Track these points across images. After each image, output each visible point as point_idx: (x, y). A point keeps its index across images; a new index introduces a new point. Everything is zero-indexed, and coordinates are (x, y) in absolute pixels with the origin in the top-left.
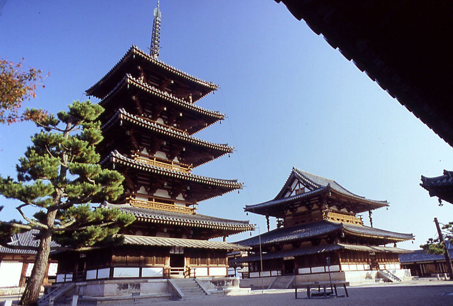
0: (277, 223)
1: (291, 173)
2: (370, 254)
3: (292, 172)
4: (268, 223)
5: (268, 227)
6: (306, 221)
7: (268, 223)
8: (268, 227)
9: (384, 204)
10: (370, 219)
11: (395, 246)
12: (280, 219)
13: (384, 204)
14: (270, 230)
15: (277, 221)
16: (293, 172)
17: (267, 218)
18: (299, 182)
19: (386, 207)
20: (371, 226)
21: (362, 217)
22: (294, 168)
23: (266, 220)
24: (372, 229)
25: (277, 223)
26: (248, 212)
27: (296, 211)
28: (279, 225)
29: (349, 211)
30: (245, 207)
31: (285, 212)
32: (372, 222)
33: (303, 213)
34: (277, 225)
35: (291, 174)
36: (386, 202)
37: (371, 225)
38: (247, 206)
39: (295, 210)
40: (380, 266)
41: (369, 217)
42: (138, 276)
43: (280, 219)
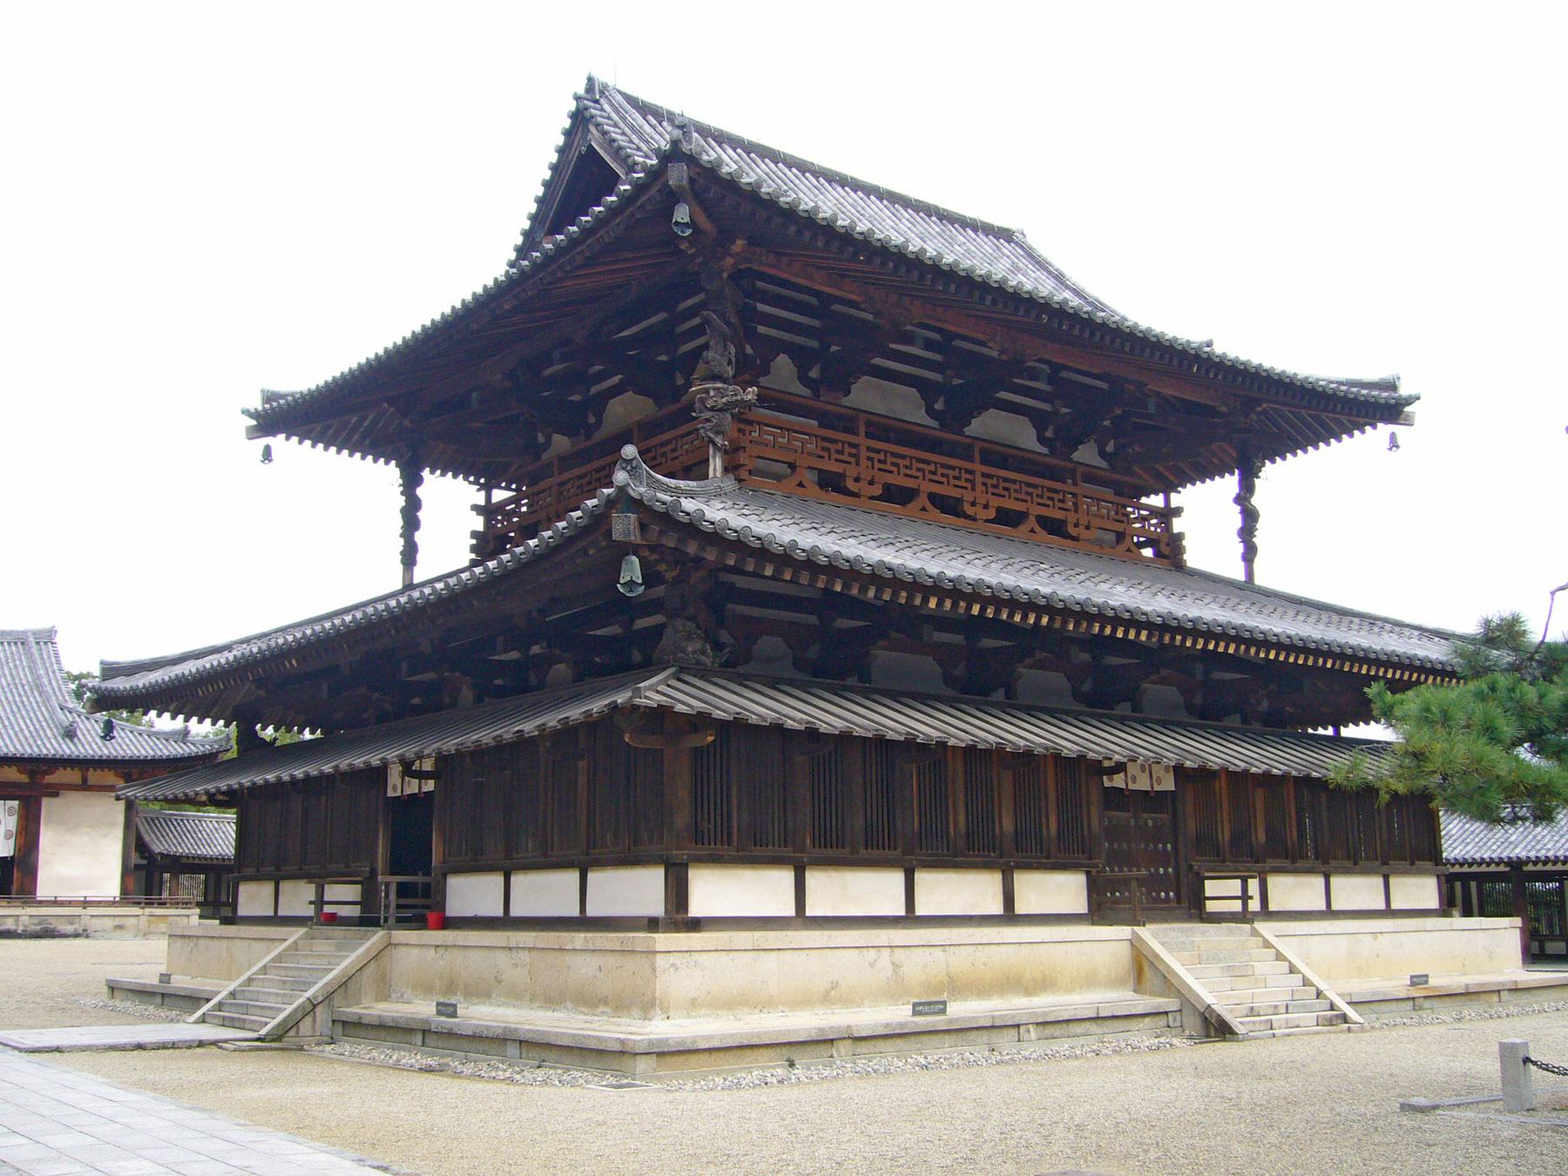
0: (478, 523)
4: (411, 521)
5: (409, 556)
7: (411, 521)
8: (409, 556)
9: (1376, 406)
10: (1237, 522)
12: (499, 495)
13: (1376, 406)
15: (475, 508)
17: (411, 482)
19: (1384, 429)
23: (401, 501)
24: (1247, 590)
25: (478, 523)
26: (278, 442)
27: (599, 423)
28: (487, 545)
29: (1064, 439)
31: (541, 439)
34: (474, 534)
36: (1392, 386)
37: (1242, 565)
39: (592, 420)
42: (903, 913)
43: (499, 495)
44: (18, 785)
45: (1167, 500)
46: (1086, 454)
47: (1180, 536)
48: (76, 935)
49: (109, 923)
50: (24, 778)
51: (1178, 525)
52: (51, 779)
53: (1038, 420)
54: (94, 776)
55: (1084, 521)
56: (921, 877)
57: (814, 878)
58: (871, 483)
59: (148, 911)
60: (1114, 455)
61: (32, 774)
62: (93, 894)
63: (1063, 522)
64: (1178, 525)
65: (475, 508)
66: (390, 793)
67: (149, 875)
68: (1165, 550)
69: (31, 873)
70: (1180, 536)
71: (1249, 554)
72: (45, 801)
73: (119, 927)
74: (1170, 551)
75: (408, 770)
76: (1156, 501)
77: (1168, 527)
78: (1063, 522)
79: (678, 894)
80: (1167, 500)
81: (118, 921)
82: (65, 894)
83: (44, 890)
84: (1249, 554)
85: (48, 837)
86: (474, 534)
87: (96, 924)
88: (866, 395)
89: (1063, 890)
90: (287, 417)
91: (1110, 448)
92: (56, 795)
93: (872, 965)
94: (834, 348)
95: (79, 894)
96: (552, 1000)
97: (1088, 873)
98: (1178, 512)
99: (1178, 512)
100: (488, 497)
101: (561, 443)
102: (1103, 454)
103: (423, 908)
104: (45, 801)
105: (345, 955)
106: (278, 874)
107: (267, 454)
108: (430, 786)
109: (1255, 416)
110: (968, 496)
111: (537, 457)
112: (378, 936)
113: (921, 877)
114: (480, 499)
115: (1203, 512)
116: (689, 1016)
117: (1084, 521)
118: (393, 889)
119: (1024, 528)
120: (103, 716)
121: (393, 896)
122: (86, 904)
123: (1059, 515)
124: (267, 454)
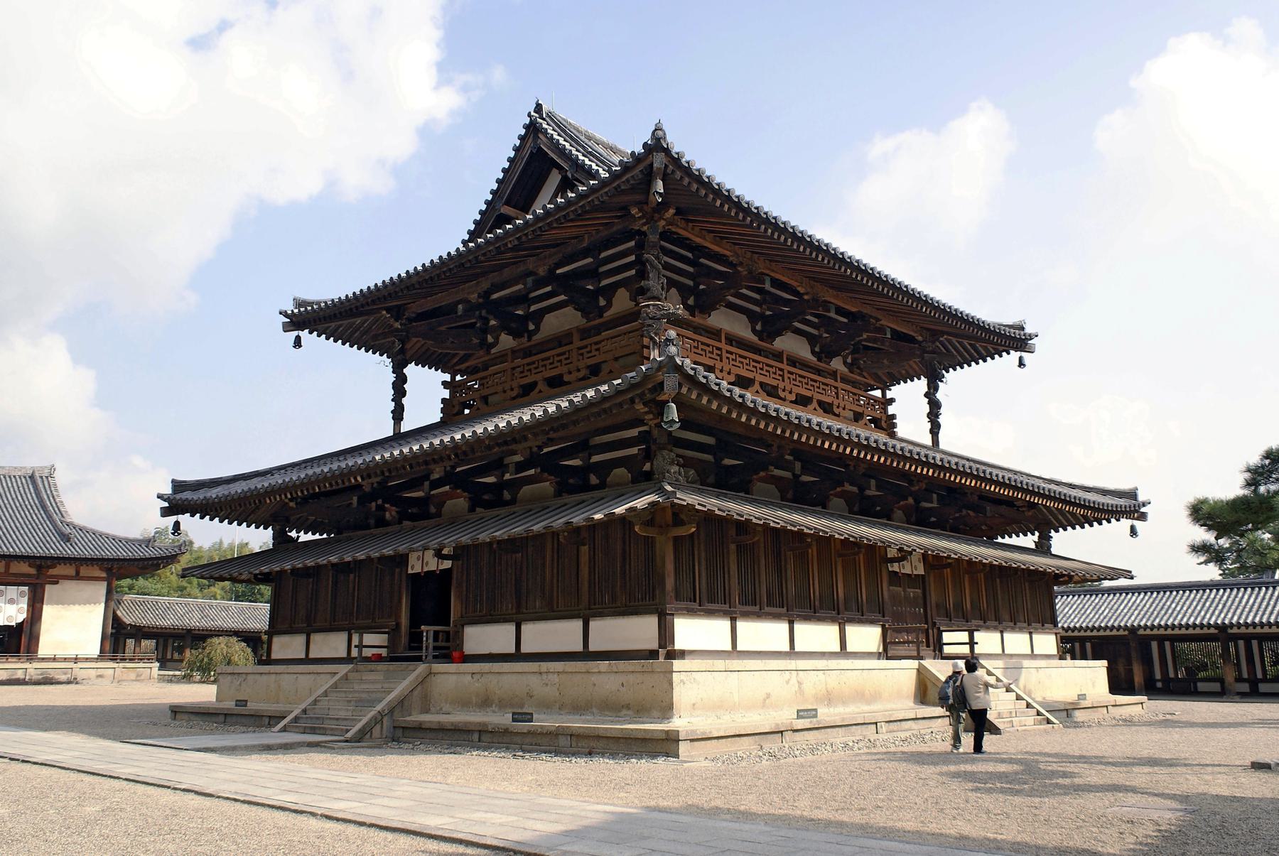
0: (446, 394)
1: (523, 132)
2: (895, 567)
3: (527, 127)
5: (398, 414)
6: (566, 378)
8: (398, 414)
9: (1011, 340)
10: (927, 409)
11: (1043, 547)
13: (1011, 340)
14: (406, 426)
15: (445, 384)
16: (532, 129)
18: (566, 184)
19: (1015, 355)
20: (928, 441)
21: (889, 395)
22: (539, 108)
23: (392, 378)
25: (446, 394)
26: (304, 334)
27: (537, 329)
29: (826, 353)
30: (290, 307)
31: (490, 339)
32: (941, 420)
33: (562, 340)
34: (444, 401)
35: (522, 138)
38: (300, 303)
39: (531, 327)
40: (947, 637)
41: (926, 395)
44: (29, 575)
45: (884, 394)
46: (837, 364)
47: (893, 416)
48: (69, 682)
49: (93, 673)
50: (33, 571)
51: (891, 410)
52: (52, 572)
53: (812, 340)
54: (84, 571)
55: (842, 405)
56: (798, 627)
57: (742, 625)
58: (729, 373)
60: (852, 364)
61: (39, 568)
62: (82, 653)
63: (831, 405)
64: (891, 410)
65: (445, 384)
66: (410, 571)
67: (119, 638)
68: (884, 425)
69: (34, 639)
70: (893, 416)
71: (935, 429)
72: (48, 587)
73: (100, 676)
74: (887, 424)
75: (439, 555)
76: (877, 393)
77: (885, 410)
78: (831, 405)
79: (666, 634)
80: (884, 394)
81: (100, 672)
82: (60, 653)
83: (44, 649)
84: (935, 429)
85: (48, 611)
86: (444, 401)
87: (81, 674)
88: (720, 319)
89: (866, 637)
90: (309, 319)
91: (849, 360)
92: (57, 583)
93: (788, 682)
94: (702, 287)
95: (71, 653)
96: (578, 708)
97: (883, 626)
98: (892, 401)
99: (892, 401)
100: (453, 378)
101: (507, 341)
102: (845, 363)
103: (450, 651)
104: (48, 587)
105: (405, 680)
106: (309, 626)
107: (298, 343)
108: (447, 564)
109: (945, 340)
110: (781, 385)
111: (488, 352)
112: (421, 668)
113: (798, 627)
114: (447, 377)
115: (907, 401)
116: (692, 716)
117: (842, 405)
118: (431, 634)
119: (811, 407)
120: (173, 519)
121: (431, 641)
122: (76, 660)
123: (829, 400)
124: (298, 343)
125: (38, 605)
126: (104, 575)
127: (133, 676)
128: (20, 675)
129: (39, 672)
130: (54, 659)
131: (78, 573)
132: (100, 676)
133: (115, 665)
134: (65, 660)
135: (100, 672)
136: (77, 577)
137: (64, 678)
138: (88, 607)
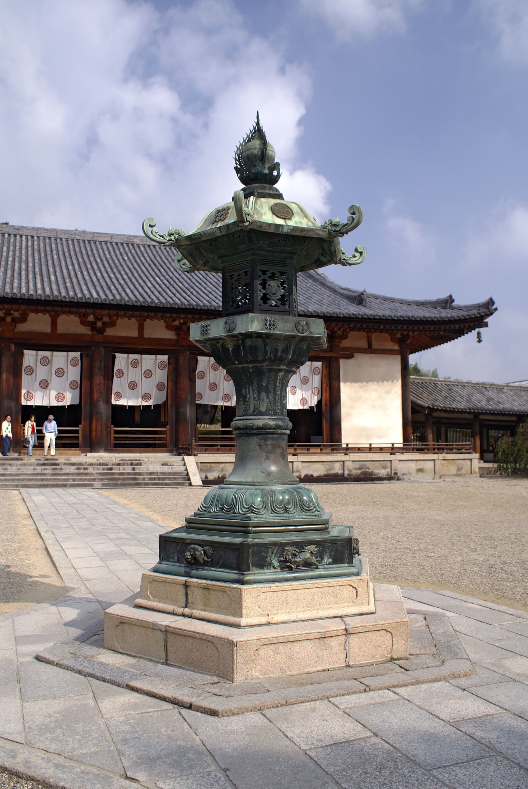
48: (389, 478)
49: (413, 466)
52: (345, 343)
59: (441, 456)
67: (431, 424)
73: (420, 470)
81: (420, 465)
83: (347, 438)
122: (393, 450)
125: (334, 383)
126: (396, 347)
127: (453, 470)
128: (337, 469)
129: (357, 465)
130: (370, 449)
131: (370, 345)
132: (420, 470)
133: (435, 457)
134: (381, 450)
135: (420, 465)
136: (370, 350)
137: (383, 473)
138: (387, 385)
